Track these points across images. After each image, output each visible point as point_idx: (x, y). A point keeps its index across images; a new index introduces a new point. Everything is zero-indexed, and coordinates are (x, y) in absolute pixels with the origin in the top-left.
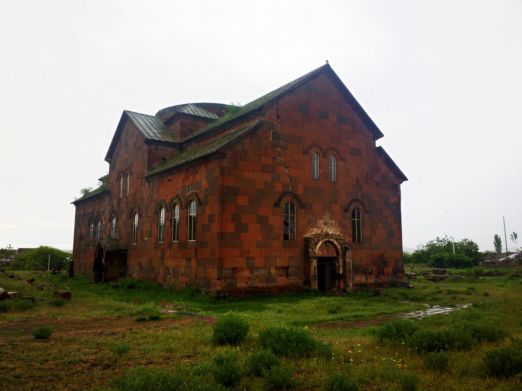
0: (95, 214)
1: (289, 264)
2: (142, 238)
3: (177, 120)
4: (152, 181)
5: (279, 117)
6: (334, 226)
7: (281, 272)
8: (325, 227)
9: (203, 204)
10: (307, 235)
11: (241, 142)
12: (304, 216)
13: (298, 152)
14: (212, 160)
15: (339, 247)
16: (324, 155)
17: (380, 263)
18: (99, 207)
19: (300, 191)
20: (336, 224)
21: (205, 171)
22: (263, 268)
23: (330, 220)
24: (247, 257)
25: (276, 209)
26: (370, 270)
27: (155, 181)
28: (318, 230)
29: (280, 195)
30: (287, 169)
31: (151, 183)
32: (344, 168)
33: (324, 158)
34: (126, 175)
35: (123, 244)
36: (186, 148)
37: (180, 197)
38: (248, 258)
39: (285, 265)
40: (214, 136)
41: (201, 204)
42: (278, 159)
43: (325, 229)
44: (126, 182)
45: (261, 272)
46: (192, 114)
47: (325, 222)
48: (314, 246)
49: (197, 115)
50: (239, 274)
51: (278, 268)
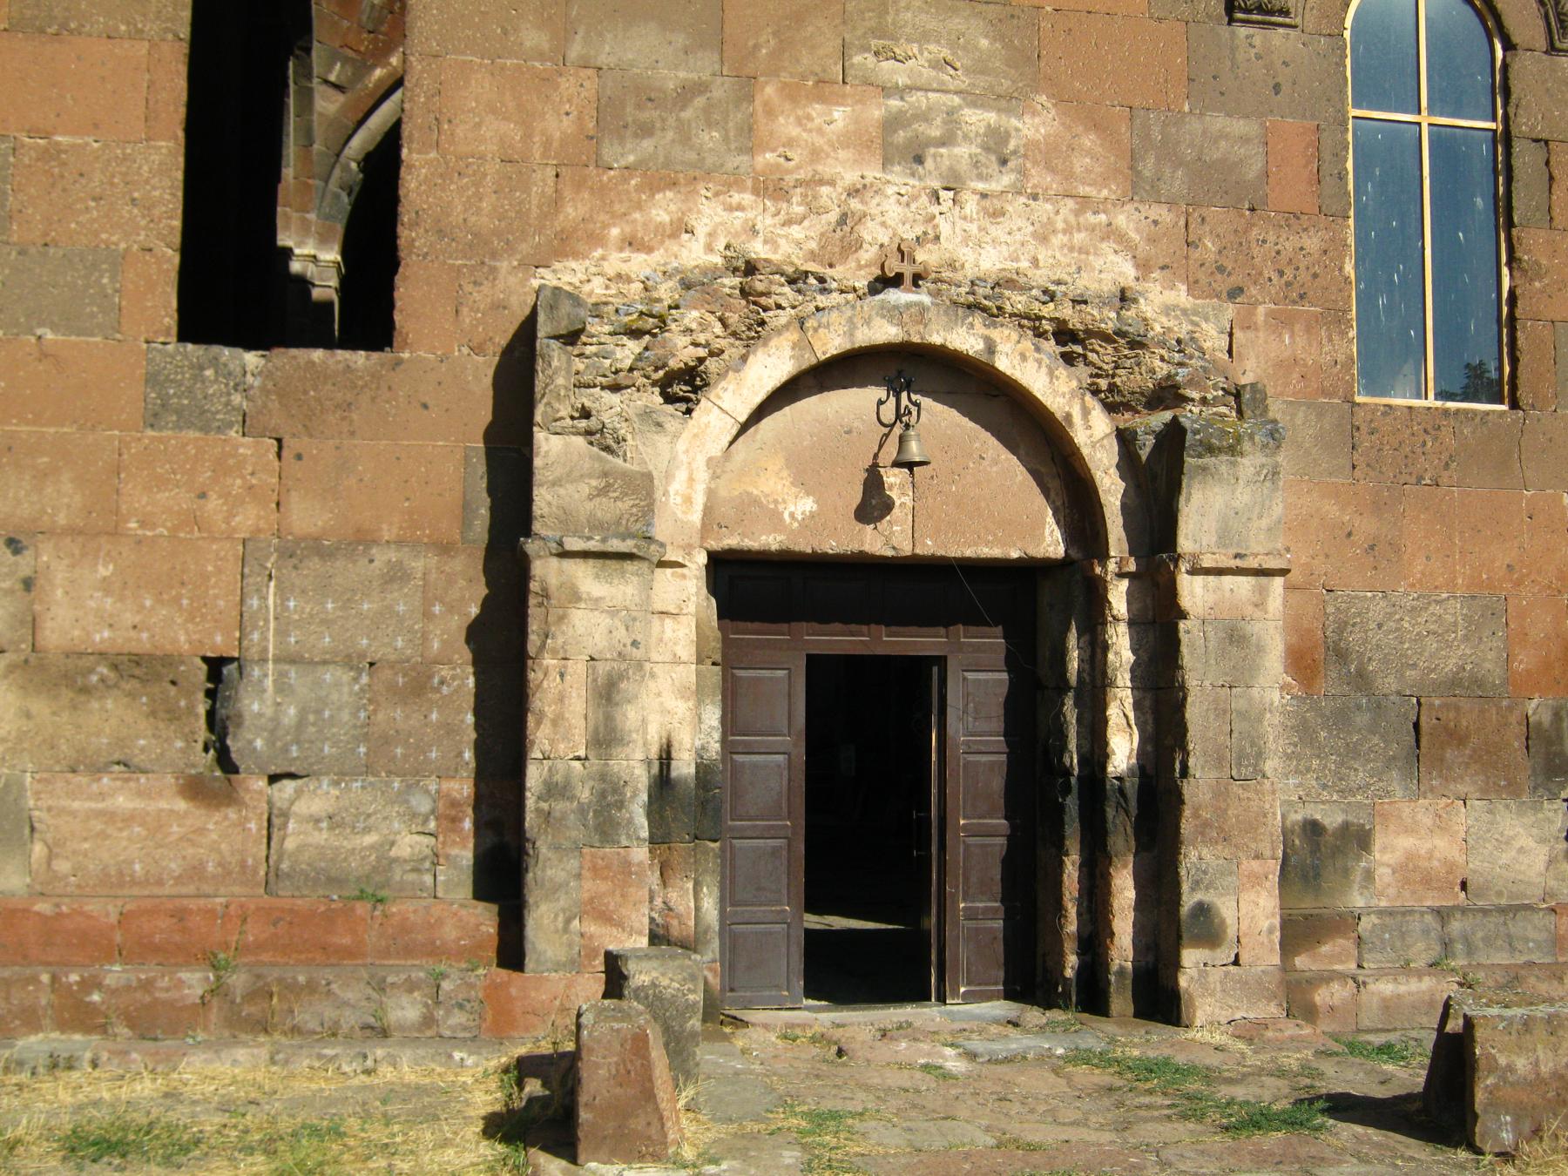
6: (1039, 177)
8: (898, 179)
10: (548, 278)
20: (1080, 163)
23: (973, 99)
43: (893, 211)
47: (892, 123)
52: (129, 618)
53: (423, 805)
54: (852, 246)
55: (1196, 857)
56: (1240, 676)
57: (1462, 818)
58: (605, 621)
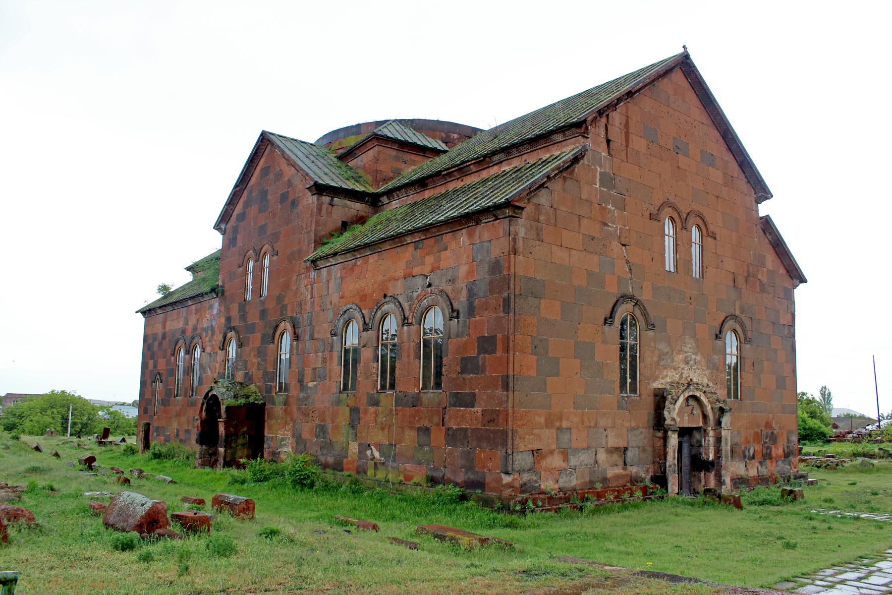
0: (189, 334)
1: (628, 443)
2: (301, 381)
3: (370, 149)
4: (325, 267)
5: (611, 142)
6: (699, 367)
7: (615, 457)
8: (686, 367)
9: (461, 315)
10: (657, 385)
11: (547, 187)
12: (653, 344)
13: (642, 215)
14: (486, 221)
15: (709, 408)
16: (682, 223)
17: (766, 439)
18: (198, 320)
19: (645, 296)
21: (467, 244)
22: (586, 451)
24: (558, 429)
25: (607, 328)
26: (752, 451)
27: (332, 267)
28: (674, 374)
29: (615, 300)
30: (624, 248)
31: (324, 272)
32: (714, 251)
33: (684, 231)
34: (261, 255)
35: (255, 393)
36: (388, 203)
37: (400, 300)
38: (559, 429)
39: (622, 444)
40: (458, 179)
41: (458, 314)
42: (611, 227)
44: (262, 270)
45: (581, 459)
46: (400, 138)
47: (686, 357)
48: (671, 406)
49: (410, 141)
50: (544, 463)
51: (611, 451)
52: (616, 441)
53: (644, 469)
54: (682, 378)
55: (723, 472)
56: (726, 444)
57: (737, 464)
58: (674, 440)
